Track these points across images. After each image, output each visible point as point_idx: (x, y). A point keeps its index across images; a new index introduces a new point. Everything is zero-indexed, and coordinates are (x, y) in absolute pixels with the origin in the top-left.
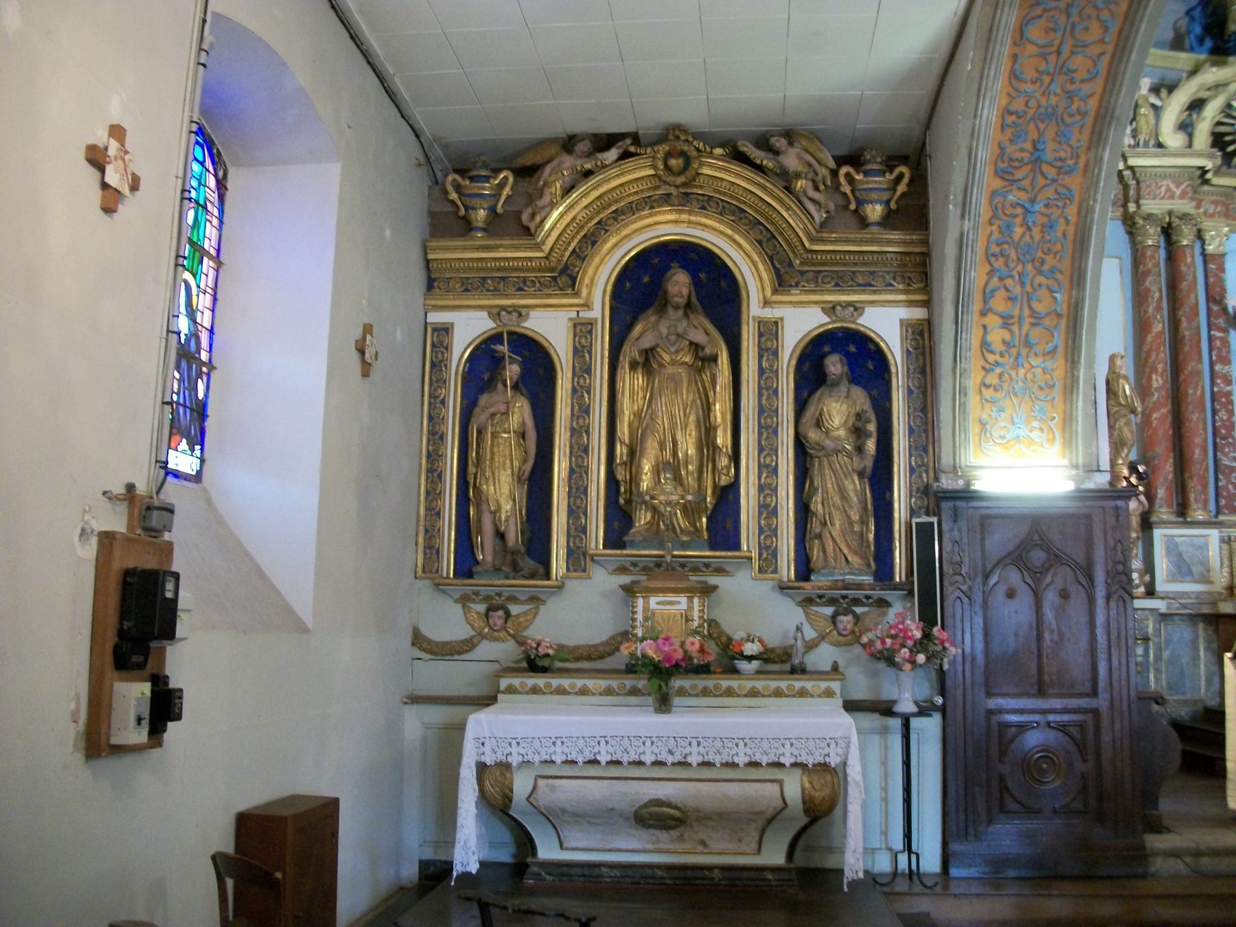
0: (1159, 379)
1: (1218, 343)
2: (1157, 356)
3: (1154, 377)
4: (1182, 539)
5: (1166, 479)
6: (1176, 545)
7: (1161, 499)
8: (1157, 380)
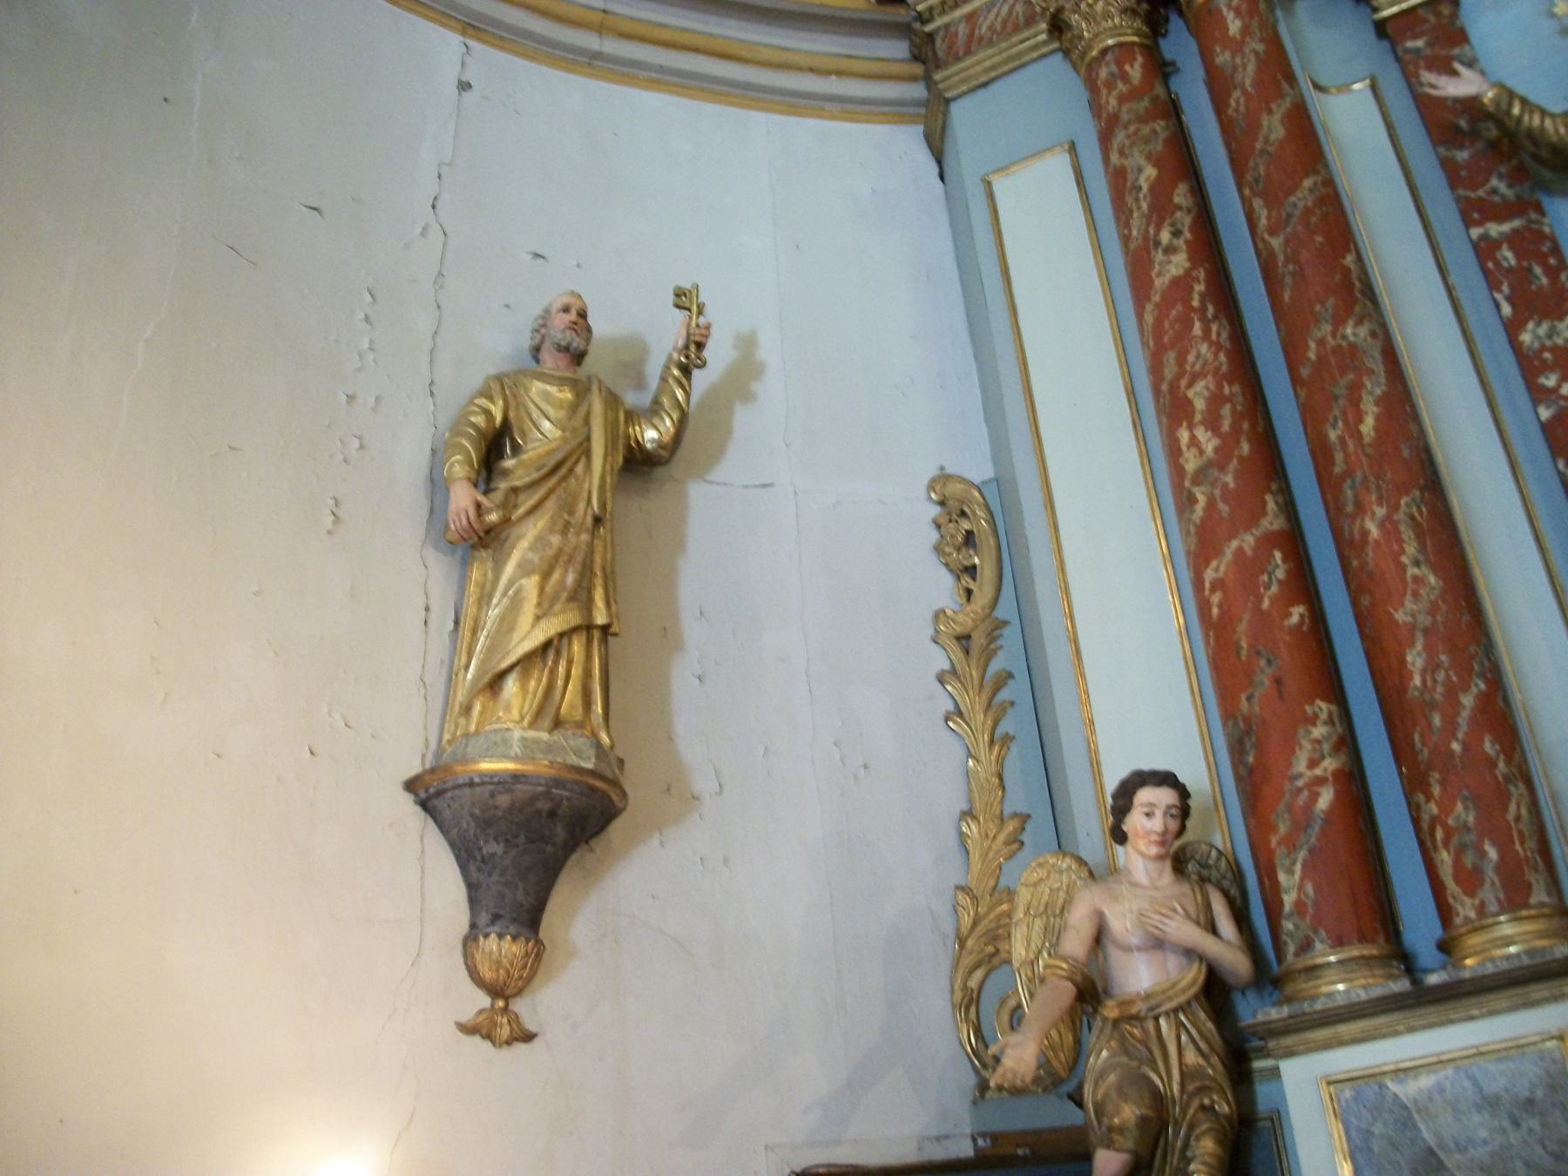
0: (1202, 434)
1: (1508, 256)
2: (1181, 361)
3: (1184, 435)
4: (1426, 1081)
5: (1302, 821)
6: (1404, 1117)
7: (1300, 906)
8: (1193, 438)
